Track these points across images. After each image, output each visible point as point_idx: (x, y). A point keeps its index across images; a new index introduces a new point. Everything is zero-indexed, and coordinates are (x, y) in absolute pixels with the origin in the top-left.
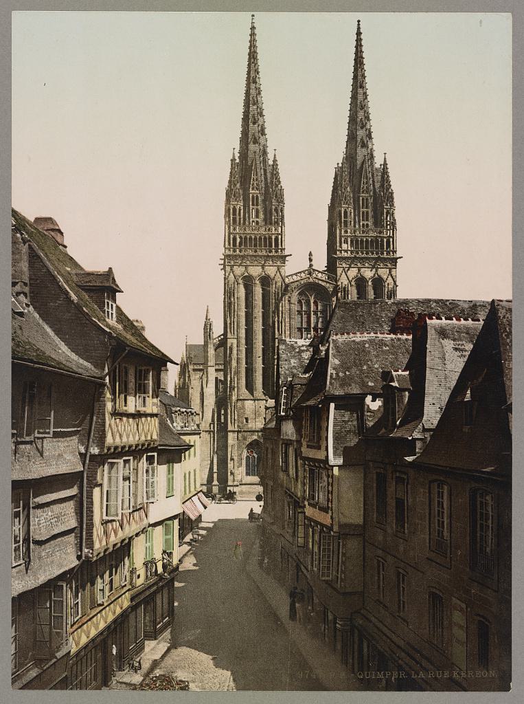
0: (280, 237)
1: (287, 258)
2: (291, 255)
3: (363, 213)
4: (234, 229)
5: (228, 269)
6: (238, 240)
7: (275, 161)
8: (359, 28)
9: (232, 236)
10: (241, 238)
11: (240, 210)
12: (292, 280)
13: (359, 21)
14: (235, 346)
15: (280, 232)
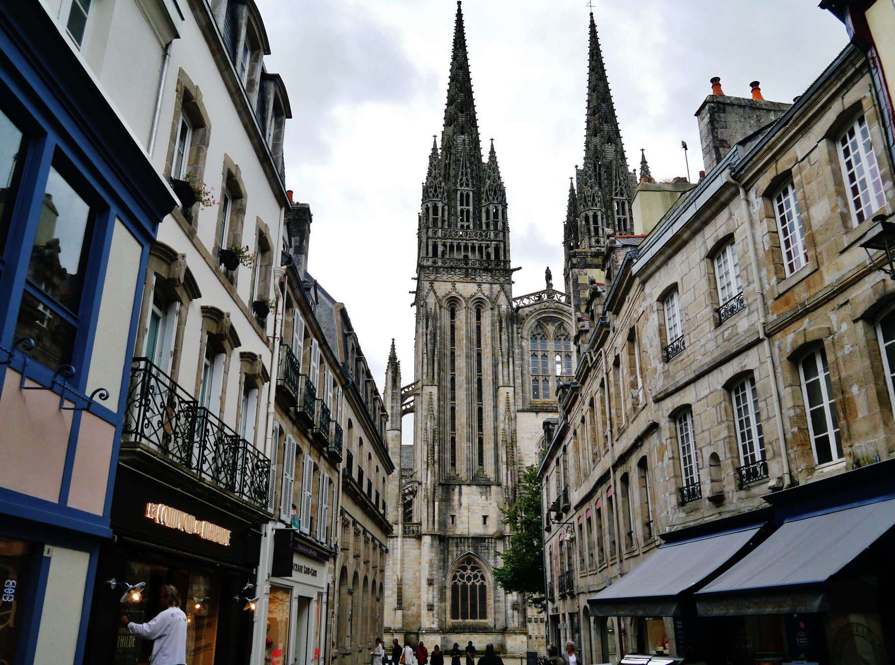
0: (502, 245)
1: (515, 276)
2: (520, 268)
3: (619, 220)
4: (435, 233)
5: (426, 285)
6: (440, 249)
7: (492, 152)
8: (592, 21)
9: (430, 242)
10: (444, 245)
11: (443, 210)
12: (522, 304)
13: (591, 14)
14: (435, 398)
15: (501, 238)
